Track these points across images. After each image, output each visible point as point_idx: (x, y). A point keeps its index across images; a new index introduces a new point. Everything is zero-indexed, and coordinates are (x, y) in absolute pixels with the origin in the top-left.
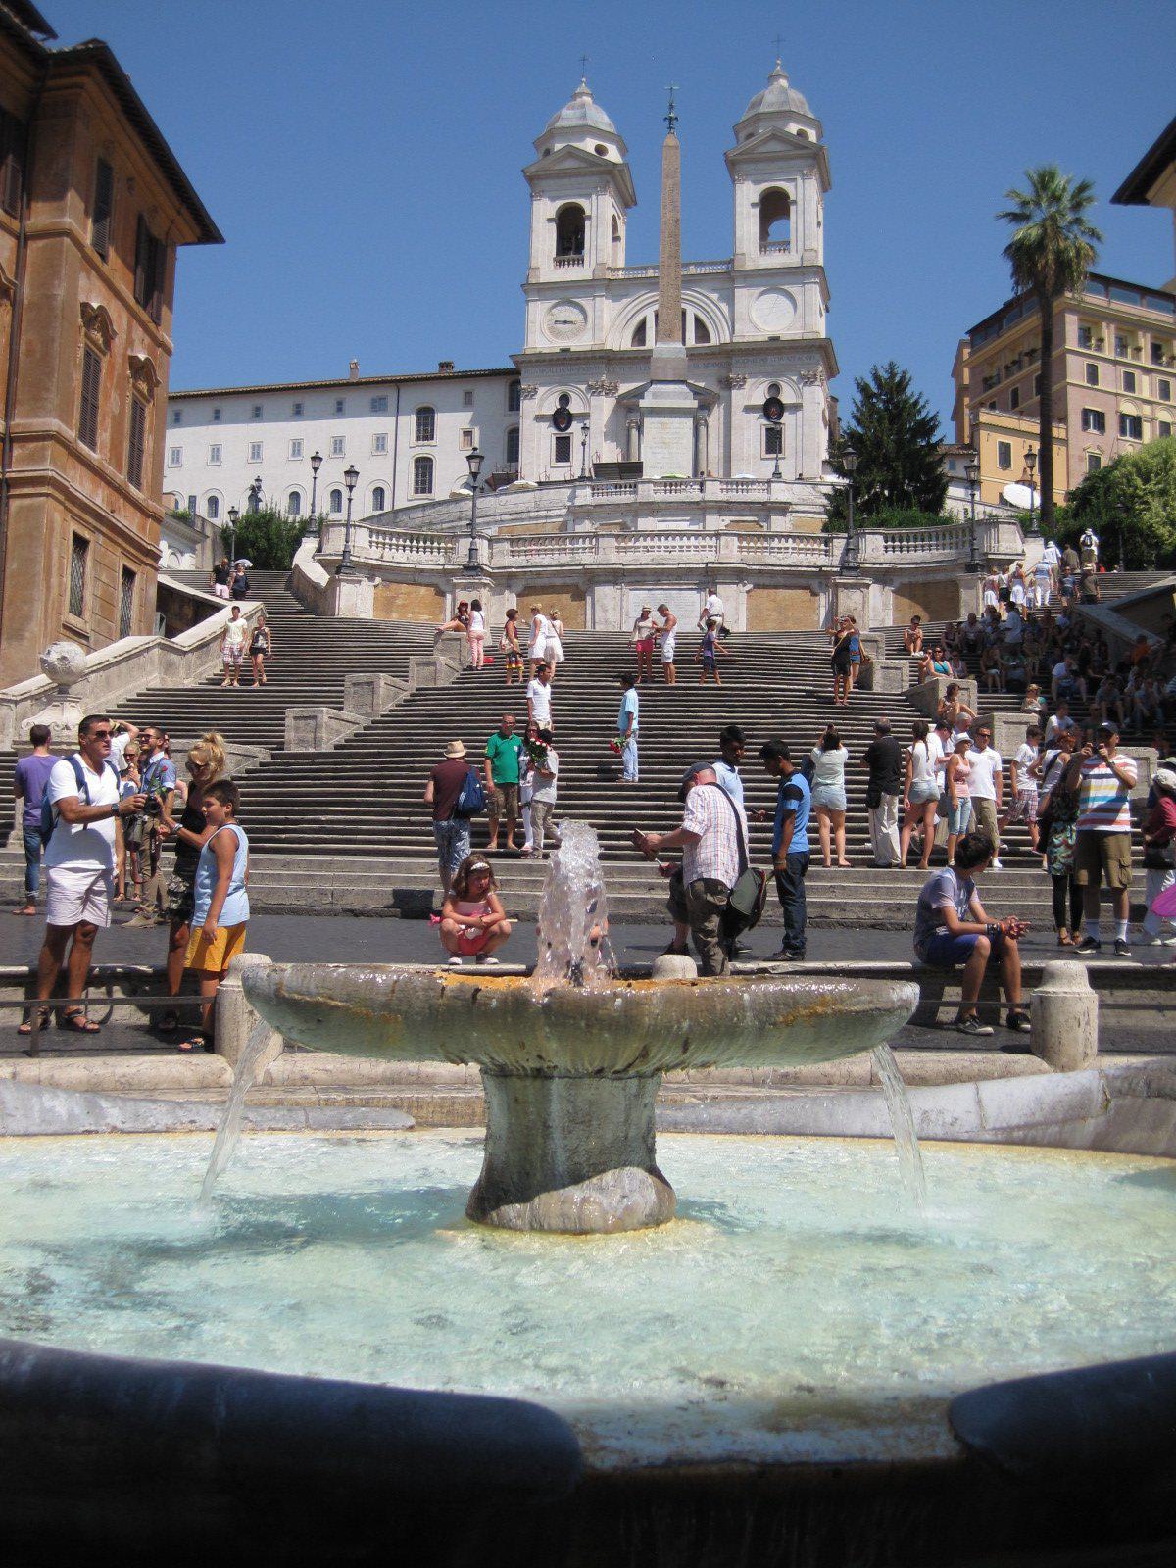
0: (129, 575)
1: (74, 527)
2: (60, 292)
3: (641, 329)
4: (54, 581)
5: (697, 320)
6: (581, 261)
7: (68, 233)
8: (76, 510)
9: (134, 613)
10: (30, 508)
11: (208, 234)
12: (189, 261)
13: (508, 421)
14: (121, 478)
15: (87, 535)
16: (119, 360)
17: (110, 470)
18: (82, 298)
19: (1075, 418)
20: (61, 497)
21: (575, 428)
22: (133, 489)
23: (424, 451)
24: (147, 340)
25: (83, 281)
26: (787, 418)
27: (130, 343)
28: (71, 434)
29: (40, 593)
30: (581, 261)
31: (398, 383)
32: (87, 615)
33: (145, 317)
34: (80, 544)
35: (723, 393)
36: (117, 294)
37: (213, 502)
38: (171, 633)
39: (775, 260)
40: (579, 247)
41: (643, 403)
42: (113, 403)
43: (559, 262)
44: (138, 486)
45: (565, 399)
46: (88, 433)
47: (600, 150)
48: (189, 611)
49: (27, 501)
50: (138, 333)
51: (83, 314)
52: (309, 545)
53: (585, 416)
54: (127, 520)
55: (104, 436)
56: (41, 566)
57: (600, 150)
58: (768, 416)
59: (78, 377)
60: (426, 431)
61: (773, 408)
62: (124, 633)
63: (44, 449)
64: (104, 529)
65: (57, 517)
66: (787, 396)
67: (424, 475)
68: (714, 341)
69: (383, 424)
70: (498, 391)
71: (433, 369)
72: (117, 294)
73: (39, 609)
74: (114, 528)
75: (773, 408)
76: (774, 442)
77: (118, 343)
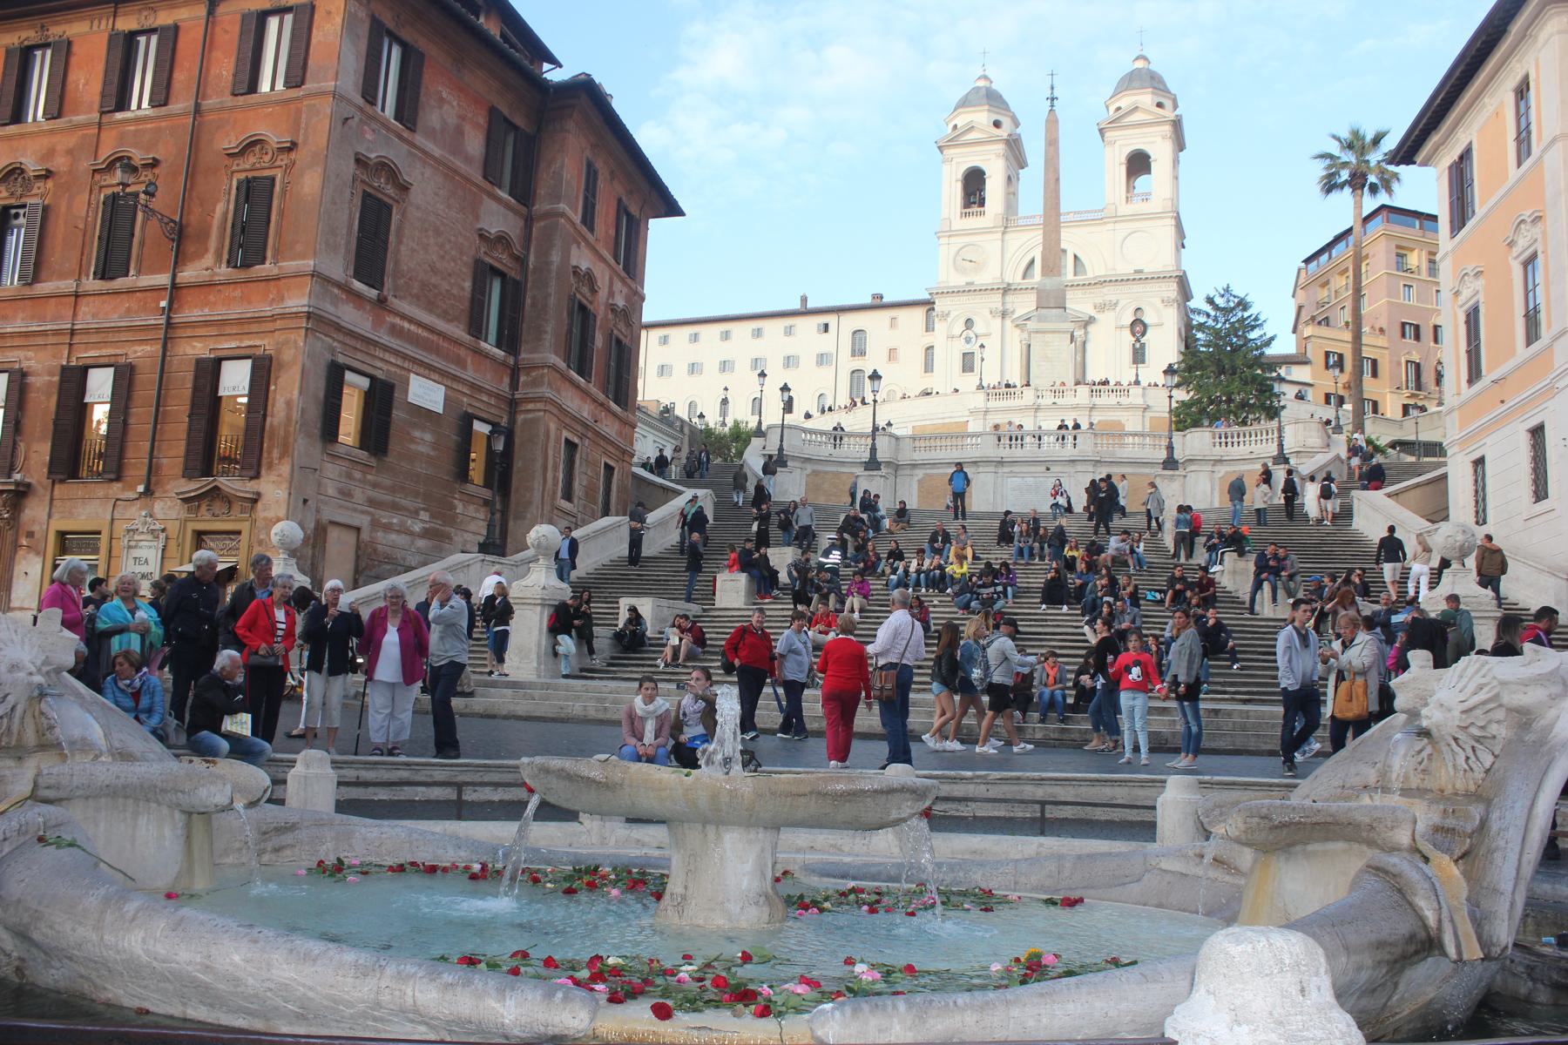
1: (565, 434)
4: (550, 475)
7: (563, 215)
8: (568, 421)
15: (576, 440)
18: (574, 262)
20: (555, 411)
24: (625, 290)
25: (574, 251)
27: (611, 294)
29: (537, 485)
33: (623, 274)
49: (530, 416)
50: (618, 285)
51: (575, 273)
52: (756, 442)
54: (609, 428)
56: (539, 464)
62: (606, 513)
63: (542, 376)
64: (590, 434)
65: (553, 426)
73: (537, 495)
74: (597, 433)
77: (603, 294)
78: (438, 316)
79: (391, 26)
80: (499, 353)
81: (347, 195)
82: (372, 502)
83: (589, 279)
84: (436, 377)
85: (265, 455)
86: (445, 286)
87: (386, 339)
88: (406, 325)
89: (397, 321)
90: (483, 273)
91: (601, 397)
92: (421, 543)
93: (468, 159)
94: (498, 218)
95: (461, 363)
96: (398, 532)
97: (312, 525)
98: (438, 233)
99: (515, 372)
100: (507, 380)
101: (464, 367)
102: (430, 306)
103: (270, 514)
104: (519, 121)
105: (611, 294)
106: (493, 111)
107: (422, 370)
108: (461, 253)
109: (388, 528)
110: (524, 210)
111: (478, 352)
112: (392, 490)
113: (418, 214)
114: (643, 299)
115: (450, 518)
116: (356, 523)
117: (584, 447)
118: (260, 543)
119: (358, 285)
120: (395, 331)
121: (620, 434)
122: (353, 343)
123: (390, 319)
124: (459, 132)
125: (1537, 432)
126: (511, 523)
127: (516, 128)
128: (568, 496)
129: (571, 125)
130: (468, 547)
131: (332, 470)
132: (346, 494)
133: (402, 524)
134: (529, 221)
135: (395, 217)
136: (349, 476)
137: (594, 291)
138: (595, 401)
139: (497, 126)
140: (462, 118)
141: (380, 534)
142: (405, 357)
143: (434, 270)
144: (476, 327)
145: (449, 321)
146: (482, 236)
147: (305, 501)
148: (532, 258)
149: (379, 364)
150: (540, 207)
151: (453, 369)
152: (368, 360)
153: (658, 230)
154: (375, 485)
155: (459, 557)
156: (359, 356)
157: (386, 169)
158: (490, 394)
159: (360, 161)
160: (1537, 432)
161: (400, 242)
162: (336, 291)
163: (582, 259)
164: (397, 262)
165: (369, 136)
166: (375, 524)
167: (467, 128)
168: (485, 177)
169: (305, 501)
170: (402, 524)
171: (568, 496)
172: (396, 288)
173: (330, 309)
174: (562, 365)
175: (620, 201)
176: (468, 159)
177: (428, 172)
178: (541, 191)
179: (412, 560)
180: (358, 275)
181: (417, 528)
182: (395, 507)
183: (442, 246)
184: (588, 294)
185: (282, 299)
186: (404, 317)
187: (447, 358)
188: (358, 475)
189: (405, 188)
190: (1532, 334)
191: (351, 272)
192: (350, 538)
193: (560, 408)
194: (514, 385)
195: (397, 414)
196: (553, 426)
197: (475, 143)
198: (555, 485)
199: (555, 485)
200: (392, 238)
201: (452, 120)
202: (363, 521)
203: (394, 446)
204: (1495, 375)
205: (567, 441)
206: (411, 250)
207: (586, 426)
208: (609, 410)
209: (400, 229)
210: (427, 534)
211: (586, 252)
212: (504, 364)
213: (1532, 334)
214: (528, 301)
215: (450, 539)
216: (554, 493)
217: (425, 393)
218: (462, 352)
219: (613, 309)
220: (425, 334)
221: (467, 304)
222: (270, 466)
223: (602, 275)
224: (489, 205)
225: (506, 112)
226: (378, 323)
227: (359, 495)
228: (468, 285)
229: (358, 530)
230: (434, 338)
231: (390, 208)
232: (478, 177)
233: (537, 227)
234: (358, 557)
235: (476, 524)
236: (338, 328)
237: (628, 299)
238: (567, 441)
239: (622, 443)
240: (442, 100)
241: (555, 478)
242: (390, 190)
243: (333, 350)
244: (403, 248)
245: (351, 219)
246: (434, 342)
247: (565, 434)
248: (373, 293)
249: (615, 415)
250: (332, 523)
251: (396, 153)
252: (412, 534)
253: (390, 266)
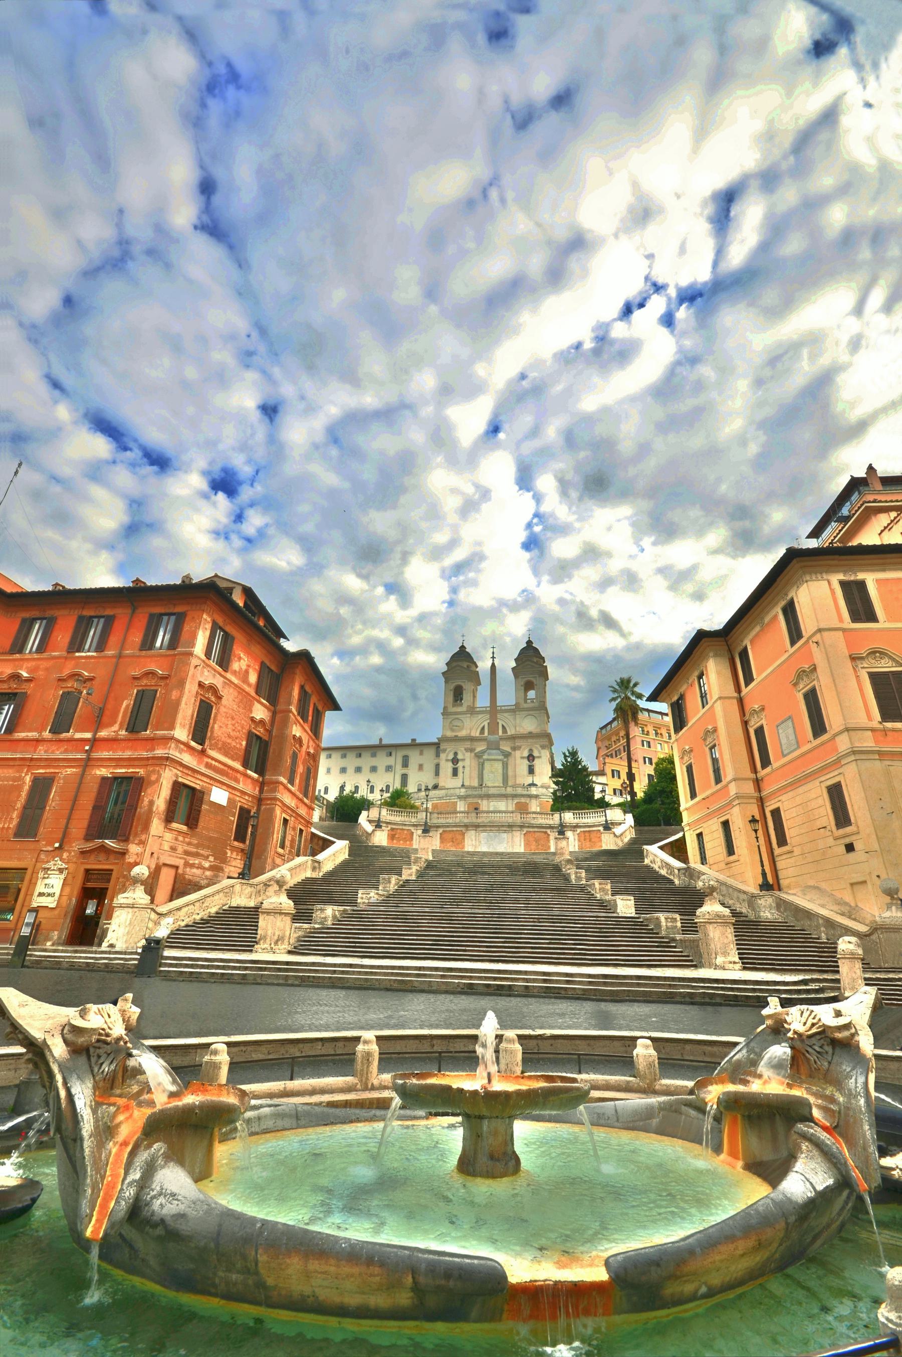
1: (284, 815)
10: (269, 809)
14: (301, 796)
15: (288, 818)
17: (298, 793)
22: (305, 800)
27: (308, 747)
34: (286, 821)
36: (305, 731)
42: (300, 769)
44: (307, 798)
46: (291, 782)
50: (311, 743)
54: (303, 811)
55: (297, 781)
62: (298, 856)
63: (276, 787)
72: (305, 731)
77: (304, 747)
78: (229, 758)
79: (221, 624)
80: (255, 776)
81: (193, 699)
82: (187, 853)
84: (225, 787)
85: (133, 829)
86: (234, 744)
87: (203, 770)
88: (213, 762)
89: (209, 760)
90: (251, 737)
91: (301, 796)
92: (208, 873)
93: (249, 685)
94: (260, 712)
95: (237, 781)
96: (198, 868)
97: (154, 867)
98: (233, 718)
99: (262, 785)
100: (257, 789)
101: (239, 783)
102: (226, 754)
103: (131, 860)
104: (273, 668)
105: (308, 747)
106: (262, 664)
107: (218, 785)
108: (243, 728)
109: (192, 866)
110: (272, 708)
111: (246, 776)
112: (197, 846)
113: (224, 710)
115: (223, 859)
116: (177, 864)
117: (292, 822)
118: (125, 877)
119: (193, 744)
120: (208, 766)
122: (187, 771)
123: (206, 760)
124: (247, 672)
125: (726, 825)
126: (253, 861)
127: (272, 671)
130: (232, 875)
131: (168, 836)
132: (173, 849)
133: (200, 863)
134: (274, 714)
135: (214, 711)
136: (176, 839)
138: (298, 798)
139: (263, 671)
140: (248, 666)
141: (188, 869)
142: (211, 778)
143: (229, 736)
144: (245, 765)
145: (234, 760)
146: (253, 719)
147: (152, 853)
148: (274, 731)
149: (198, 782)
150: (281, 707)
151: (233, 784)
152: (193, 780)
154: (189, 844)
155: (227, 882)
156: (189, 778)
157: (213, 689)
158: (249, 795)
159: (201, 685)
160: (726, 825)
161: (214, 723)
162: (182, 746)
163: (296, 731)
164: (212, 732)
165: (206, 673)
166: (187, 864)
167: (251, 671)
168: (256, 693)
169: (152, 853)
170: (200, 863)
171: (283, 847)
172: (211, 745)
173: (178, 755)
176: (249, 685)
177: (231, 690)
178: (281, 700)
179: (203, 882)
180: (193, 739)
181: (207, 865)
182: (197, 855)
183: (233, 725)
185: (154, 750)
186: (213, 759)
187: (231, 778)
188: (181, 838)
189: (219, 698)
190: (718, 780)
191: (190, 737)
192: (172, 872)
193: (282, 802)
194: (261, 791)
195: (205, 807)
197: (253, 678)
200: (211, 721)
201: (244, 667)
202: (180, 863)
203: (201, 824)
204: (704, 796)
205: (284, 819)
206: (220, 728)
209: (216, 714)
210: (211, 868)
211: (299, 728)
212: (257, 781)
213: (718, 780)
214: (271, 751)
215: (223, 870)
217: (219, 796)
218: (239, 775)
219: (308, 753)
220: (222, 767)
221: (243, 752)
222: (136, 835)
224: (257, 706)
225: (268, 664)
226: (200, 762)
227: (180, 849)
228: (244, 743)
229: (177, 868)
230: (226, 768)
231: (212, 707)
232: (253, 693)
233: (278, 717)
234: (175, 882)
235: (236, 864)
236: (181, 765)
238: (284, 819)
240: (240, 659)
242: (213, 699)
243: (177, 776)
244: (216, 726)
245: (193, 712)
246: (227, 771)
247: (284, 815)
248: (199, 747)
249: (306, 804)
250: (165, 865)
251: (218, 682)
252: (204, 869)
253: (209, 734)
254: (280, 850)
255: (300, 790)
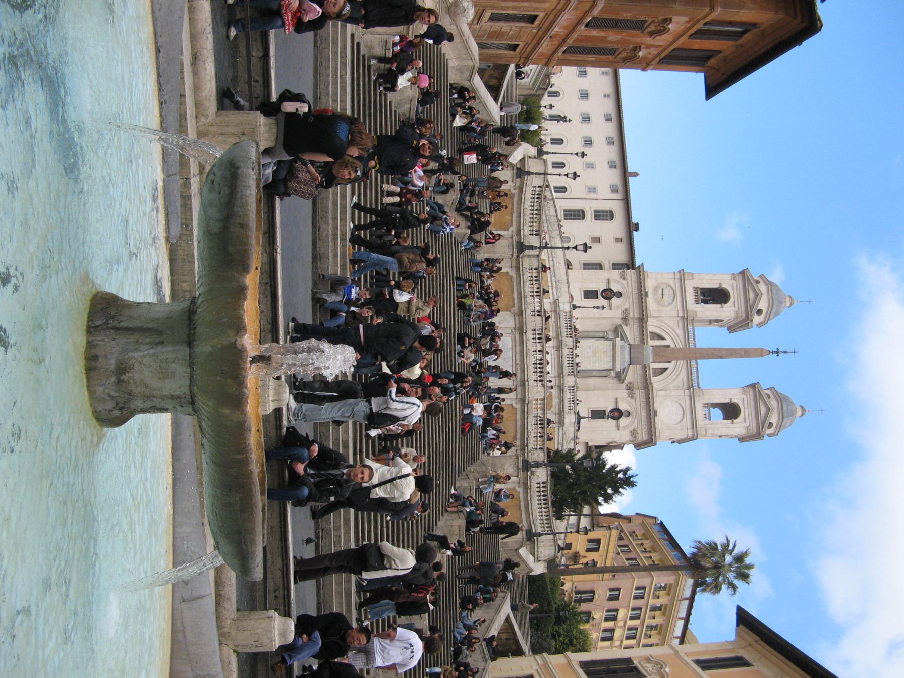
0: (514, 47)
1: (541, 15)
2: (677, 6)
3: (661, 338)
5: (666, 369)
6: (697, 302)
8: (552, 16)
9: (490, 51)
11: (711, 90)
12: (695, 80)
13: (607, 265)
14: (570, 42)
15: (537, 22)
16: (638, 40)
17: (575, 35)
18: (674, 19)
19: (614, 584)
20: (560, 7)
21: (604, 302)
23: (589, 215)
24: (650, 57)
25: (684, 19)
26: (611, 422)
27: (648, 47)
28: (595, 12)
30: (697, 302)
31: (626, 200)
32: (490, 24)
33: (663, 55)
34: (532, 19)
35: (624, 385)
37: (555, 94)
38: (481, 72)
39: (700, 412)
40: (705, 302)
41: (618, 340)
42: (613, 37)
43: (696, 289)
45: (619, 295)
47: (759, 312)
48: (493, 82)
50: (654, 51)
51: (666, 19)
52: (533, 151)
53: (610, 306)
54: (545, 47)
55: (594, 33)
57: (759, 312)
58: (612, 411)
59: (627, 15)
60: (600, 215)
61: (617, 414)
62: (481, 46)
64: (541, 33)
65: (546, 5)
66: (623, 421)
67: (574, 215)
68: (654, 380)
69: (604, 192)
70: (623, 258)
71: (634, 221)
75: (617, 414)
76: (597, 415)
77: (649, 40)
83: (661, 30)
91: (570, 42)
105: (648, 47)
114: (644, 69)
117: (532, 29)
121: (542, 55)
128: (493, 18)
129: (781, 15)
137: (651, 34)
138: (567, 36)
153: (695, 80)
174: (595, 12)
175: (720, 52)
184: (649, 30)
196: (546, 5)
198: (502, 8)
199: (502, 8)
205: (536, 16)
207: (548, 29)
208: (560, 46)
216: (496, 8)
219: (637, 48)
223: (662, 40)
237: (644, 58)
238: (536, 16)
239: (534, 56)
241: (508, 8)
247: (541, 15)
249: (556, 51)
254: (487, 15)
255: (581, 39)
